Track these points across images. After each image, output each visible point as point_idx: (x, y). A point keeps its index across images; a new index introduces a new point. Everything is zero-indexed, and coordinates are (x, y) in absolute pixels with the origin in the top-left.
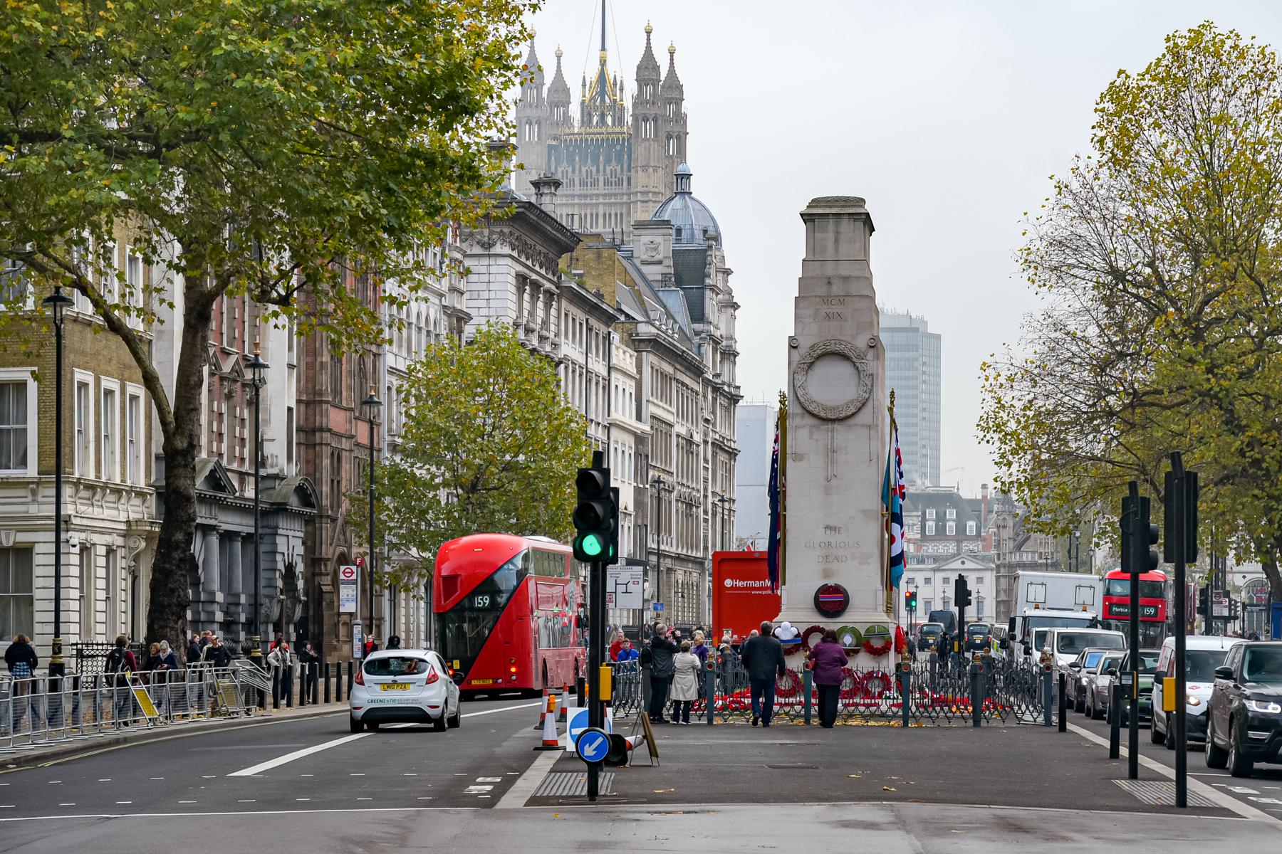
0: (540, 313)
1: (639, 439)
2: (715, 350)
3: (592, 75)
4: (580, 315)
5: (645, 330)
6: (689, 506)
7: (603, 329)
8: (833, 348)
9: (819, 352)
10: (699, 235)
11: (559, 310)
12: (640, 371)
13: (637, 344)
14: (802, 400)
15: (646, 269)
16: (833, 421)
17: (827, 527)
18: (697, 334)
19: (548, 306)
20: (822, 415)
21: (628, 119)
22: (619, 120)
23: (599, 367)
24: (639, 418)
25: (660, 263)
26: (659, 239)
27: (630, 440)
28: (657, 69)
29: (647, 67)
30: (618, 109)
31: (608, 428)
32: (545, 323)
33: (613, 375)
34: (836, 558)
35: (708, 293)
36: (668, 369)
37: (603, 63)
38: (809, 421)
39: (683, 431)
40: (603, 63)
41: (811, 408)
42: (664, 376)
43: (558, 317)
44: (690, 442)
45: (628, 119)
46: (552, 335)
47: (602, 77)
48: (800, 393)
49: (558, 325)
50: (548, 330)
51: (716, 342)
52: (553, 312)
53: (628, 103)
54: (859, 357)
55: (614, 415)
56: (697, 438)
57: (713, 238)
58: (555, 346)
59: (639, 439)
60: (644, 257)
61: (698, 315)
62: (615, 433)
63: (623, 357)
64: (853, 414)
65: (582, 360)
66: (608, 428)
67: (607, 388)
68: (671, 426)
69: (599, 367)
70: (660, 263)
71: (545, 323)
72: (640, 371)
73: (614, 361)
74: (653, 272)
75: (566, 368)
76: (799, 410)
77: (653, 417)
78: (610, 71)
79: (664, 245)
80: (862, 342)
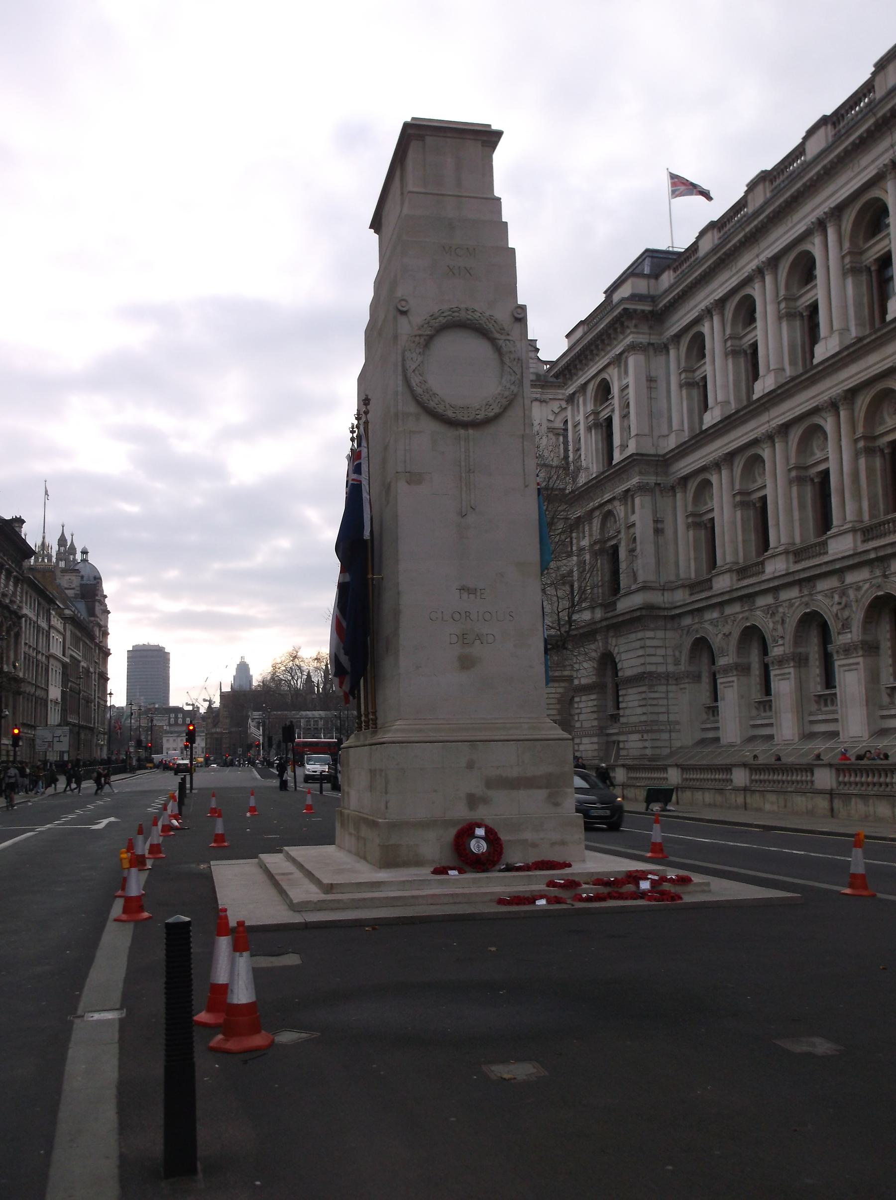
0: (11, 588)
1: (65, 666)
2: (100, 630)
3: (39, 543)
4: (34, 595)
5: (67, 612)
6: (88, 702)
7: (46, 606)
8: (463, 315)
9: (442, 320)
10: (92, 578)
11: (22, 589)
12: (65, 630)
13: (65, 619)
14: (419, 390)
15: (67, 591)
16: (465, 425)
17: (462, 589)
18: (92, 622)
19: (15, 586)
20: (450, 414)
21: (54, 560)
22: (50, 560)
23: (44, 625)
24: (64, 655)
25: (73, 589)
26: (73, 578)
27: (59, 666)
28: (66, 540)
29: (62, 541)
30: (50, 557)
31: (48, 657)
32: (14, 593)
33: (52, 631)
34: (479, 637)
35: (97, 604)
36: (80, 635)
37: (44, 538)
38: (429, 426)
39: (85, 665)
40: (44, 538)
41: (432, 404)
42: (77, 637)
43: (22, 593)
44: (88, 671)
45: (54, 560)
46: (18, 602)
47: (43, 543)
48: (415, 380)
49: (21, 597)
50: (16, 597)
51: (100, 626)
52: (19, 589)
53: (54, 554)
54: (502, 330)
55: (52, 651)
56: (92, 670)
57: (98, 580)
58: (20, 608)
59: (65, 666)
60: (66, 586)
61: (92, 612)
62: (52, 661)
63: (56, 622)
64: (497, 417)
65: (35, 619)
66: (48, 657)
67: (48, 636)
68: (79, 662)
69: (44, 625)
70: (73, 589)
71: (14, 593)
72: (65, 630)
73: (52, 623)
74: (70, 593)
75: (26, 621)
76: (412, 408)
77: (72, 656)
78: (47, 541)
79: (76, 582)
80: (502, 315)
